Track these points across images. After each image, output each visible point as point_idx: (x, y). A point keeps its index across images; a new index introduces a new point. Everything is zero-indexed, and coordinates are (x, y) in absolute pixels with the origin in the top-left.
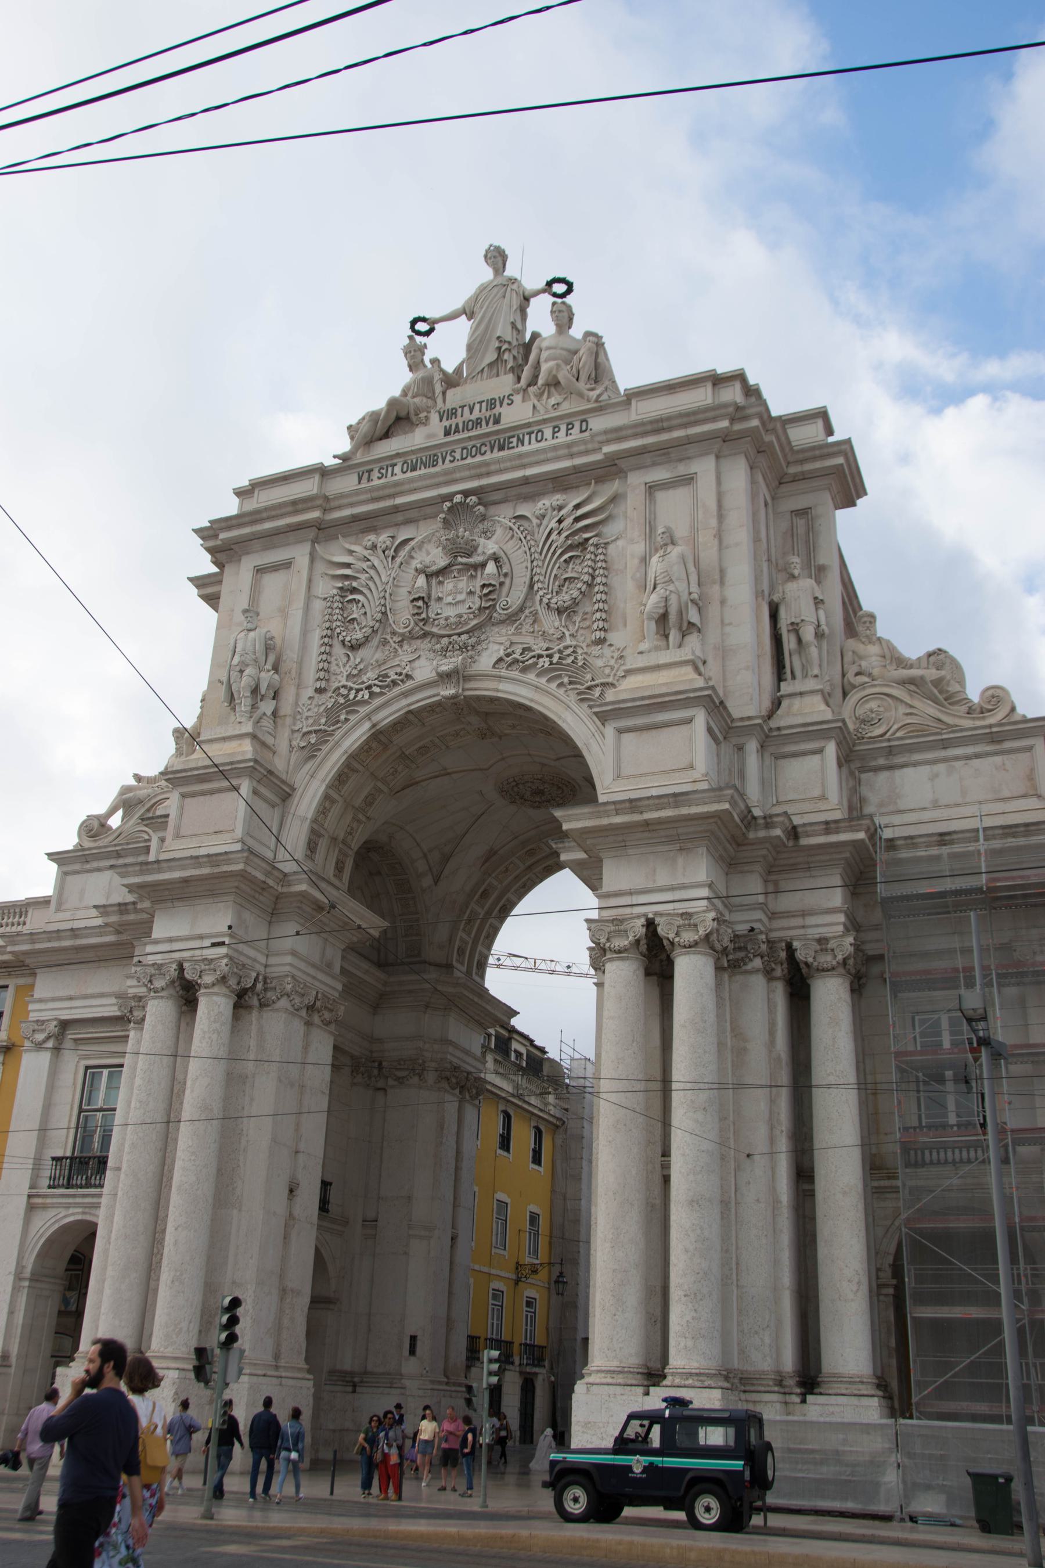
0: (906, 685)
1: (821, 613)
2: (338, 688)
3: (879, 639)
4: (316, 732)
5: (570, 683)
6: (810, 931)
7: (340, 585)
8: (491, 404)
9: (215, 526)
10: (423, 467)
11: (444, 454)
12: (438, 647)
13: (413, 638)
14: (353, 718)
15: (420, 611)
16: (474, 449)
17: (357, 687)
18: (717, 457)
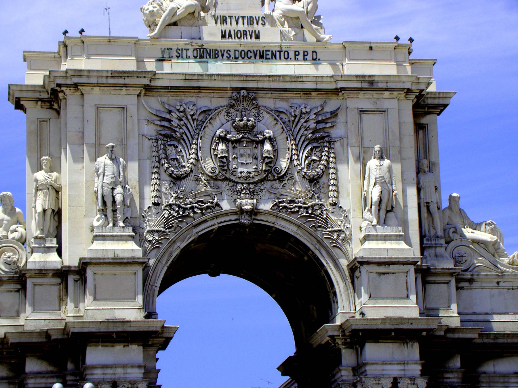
0: (480, 244)
1: (437, 193)
2: (170, 205)
3: (460, 210)
4: (158, 231)
5: (320, 227)
6: (445, 380)
7: (163, 132)
8: (251, 20)
9: (70, 73)
10: (208, 57)
11: (222, 51)
12: (234, 188)
13: (216, 180)
14: (184, 226)
15: (224, 165)
16: (243, 52)
17: (184, 206)
18: (398, 99)
